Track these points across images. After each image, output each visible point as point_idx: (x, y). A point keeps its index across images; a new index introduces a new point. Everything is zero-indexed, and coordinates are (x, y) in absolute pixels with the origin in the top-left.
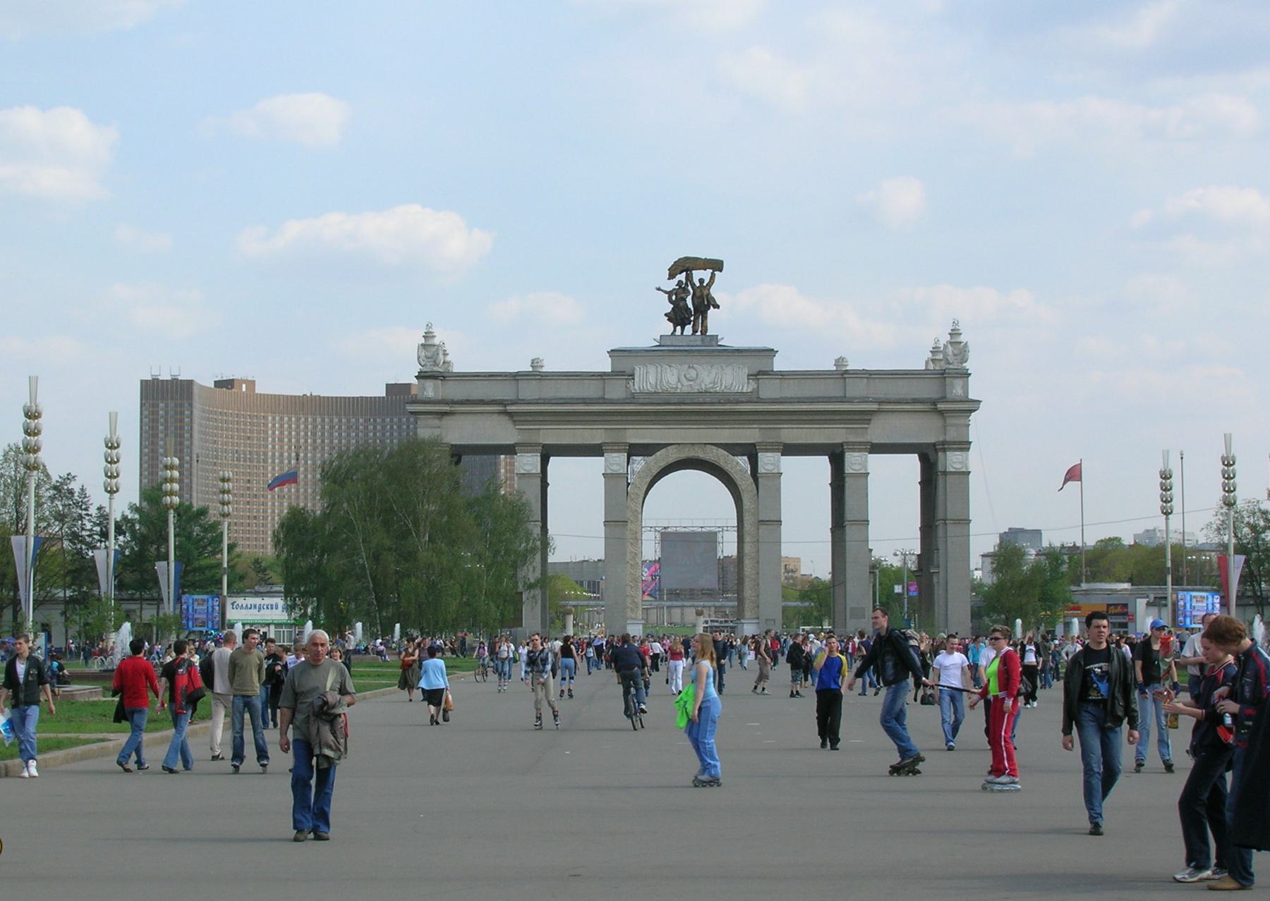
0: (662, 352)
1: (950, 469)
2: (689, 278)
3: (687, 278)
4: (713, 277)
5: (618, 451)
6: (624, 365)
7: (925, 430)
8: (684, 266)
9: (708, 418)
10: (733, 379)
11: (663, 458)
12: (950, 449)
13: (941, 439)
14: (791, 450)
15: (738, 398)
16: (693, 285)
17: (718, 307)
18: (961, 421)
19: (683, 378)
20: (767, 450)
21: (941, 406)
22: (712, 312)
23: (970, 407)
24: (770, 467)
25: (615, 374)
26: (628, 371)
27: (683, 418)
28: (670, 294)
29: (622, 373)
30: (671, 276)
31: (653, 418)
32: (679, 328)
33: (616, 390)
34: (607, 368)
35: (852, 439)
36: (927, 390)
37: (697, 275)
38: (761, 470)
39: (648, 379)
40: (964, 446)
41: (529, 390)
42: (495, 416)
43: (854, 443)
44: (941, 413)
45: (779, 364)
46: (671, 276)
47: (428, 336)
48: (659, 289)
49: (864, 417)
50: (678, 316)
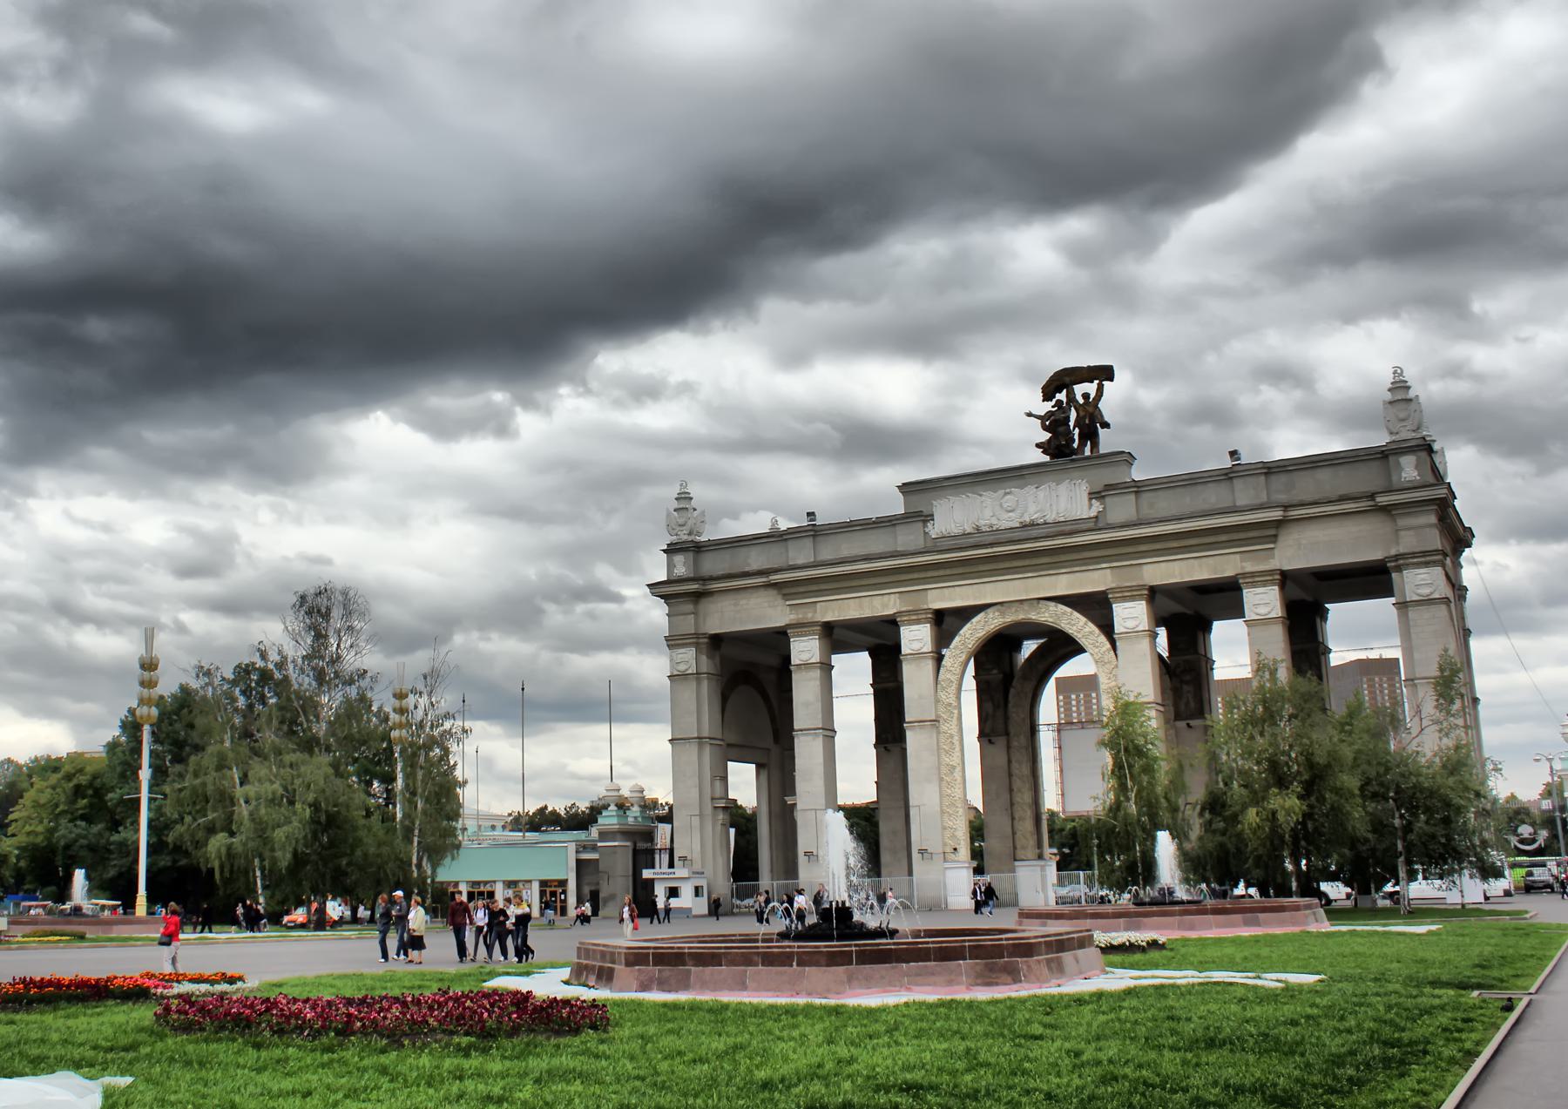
2: (1071, 398)
5: (918, 622)
6: (920, 503)
20: (1124, 599)
31: (961, 570)
35: (1249, 567)
36: (1364, 479)
37: (1079, 389)
38: (1118, 628)
41: (801, 553)
42: (762, 592)
46: (1048, 394)
48: (1030, 415)
49: (1269, 532)
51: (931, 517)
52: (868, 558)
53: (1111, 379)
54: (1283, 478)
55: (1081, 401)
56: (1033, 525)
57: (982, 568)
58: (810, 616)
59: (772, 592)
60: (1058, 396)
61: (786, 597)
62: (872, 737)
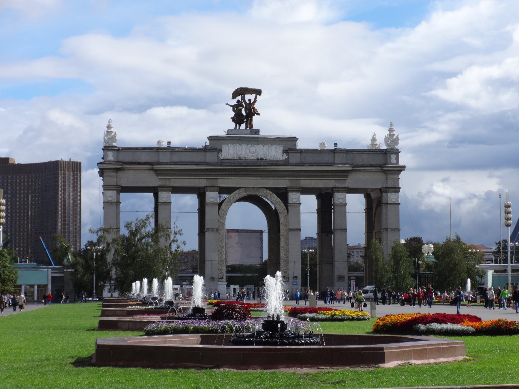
0: (230, 139)
1: (389, 202)
2: (243, 99)
3: (242, 99)
4: (256, 98)
5: (214, 191)
6: (216, 145)
7: (373, 180)
8: (241, 92)
9: (262, 173)
10: (276, 153)
11: (236, 194)
12: (389, 191)
13: (385, 186)
14: (306, 191)
17: (258, 114)
18: (395, 176)
20: (293, 191)
21: (385, 169)
22: (255, 118)
24: (294, 200)
26: (219, 148)
27: (248, 173)
28: (233, 107)
30: (234, 97)
31: (233, 173)
32: (238, 125)
35: (338, 185)
36: (378, 160)
37: (248, 97)
38: (290, 201)
39: (230, 152)
40: (397, 189)
41: (165, 157)
42: (147, 172)
43: (339, 188)
44: (385, 172)
45: (300, 145)
46: (234, 97)
47: (109, 127)
48: (227, 104)
49: (345, 174)
50: (238, 119)
51: (221, 151)
54: (352, 155)
55: (248, 102)
56: (261, 159)
57: (241, 173)
58: (168, 183)
59: (152, 173)
61: (158, 175)
62: (197, 233)
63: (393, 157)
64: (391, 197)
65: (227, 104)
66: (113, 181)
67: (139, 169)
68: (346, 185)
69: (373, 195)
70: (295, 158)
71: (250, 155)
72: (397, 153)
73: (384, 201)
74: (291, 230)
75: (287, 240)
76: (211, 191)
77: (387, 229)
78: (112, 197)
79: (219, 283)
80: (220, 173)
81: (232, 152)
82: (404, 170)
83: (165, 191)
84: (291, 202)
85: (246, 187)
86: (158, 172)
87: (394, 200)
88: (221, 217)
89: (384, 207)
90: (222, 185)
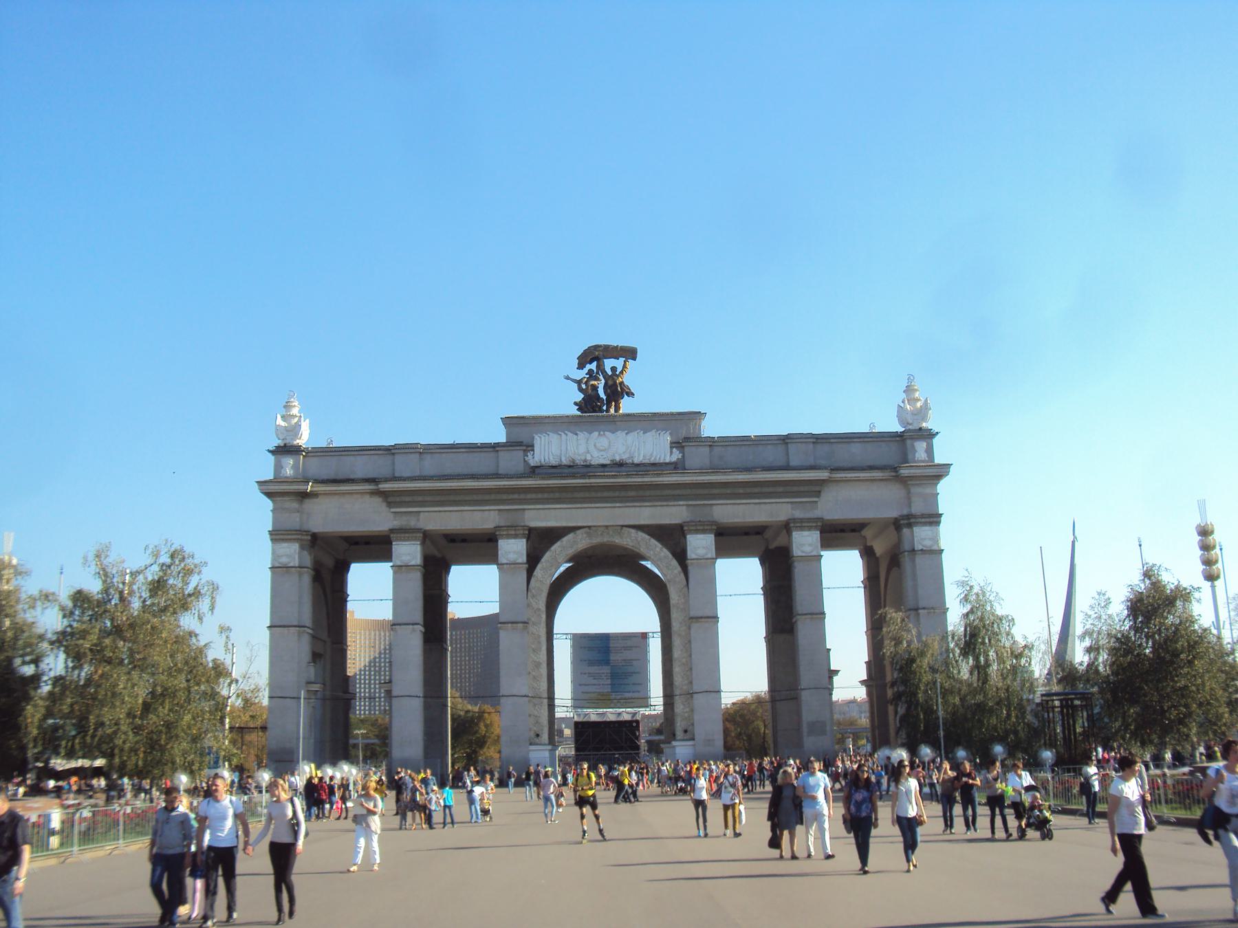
2: (600, 367)
3: (598, 367)
4: (625, 366)
5: (516, 536)
6: (522, 434)
8: (593, 355)
10: (654, 447)
12: (917, 524)
13: (905, 512)
15: (656, 467)
16: (604, 372)
17: (630, 394)
18: (928, 490)
19: (592, 448)
20: (697, 531)
21: (904, 472)
23: (940, 472)
25: (511, 444)
28: (579, 382)
29: (520, 444)
31: (557, 495)
33: (510, 461)
34: (502, 439)
35: (798, 514)
36: (887, 454)
37: (609, 364)
38: (691, 554)
41: (406, 466)
42: (368, 496)
43: (802, 520)
44: (904, 481)
45: (710, 428)
46: (581, 366)
48: (567, 378)
49: (814, 489)
50: (590, 404)
51: (530, 447)
52: (473, 477)
53: (634, 359)
55: (610, 373)
58: (413, 523)
59: (377, 501)
60: (588, 367)
63: (921, 446)
64: (921, 535)
65: (567, 378)
66: (294, 521)
67: (350, 493)
68: (817, 513)
69: (879, 548)
70: (698, 456)
71: (596, 454)
72: (929, 435)
73: (907, 547)
74: (698, 618)
75: (688, 643)
76: (509, 536)
77: (916, 609)
78: (288, 556)
79: (532, 748)
80: (529, 496)
81: (555, 449)
82: (947, 473)
83: (408, 540)
84: (694, 556)
85: (589, 527)
86: (391, 499)
87: (928, 543)
88: (533, 596)
89: (906, 560)
90: (533, 524)
